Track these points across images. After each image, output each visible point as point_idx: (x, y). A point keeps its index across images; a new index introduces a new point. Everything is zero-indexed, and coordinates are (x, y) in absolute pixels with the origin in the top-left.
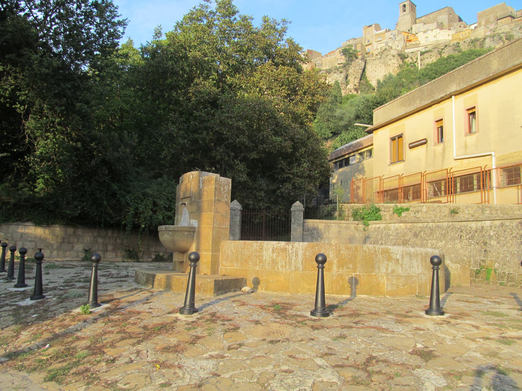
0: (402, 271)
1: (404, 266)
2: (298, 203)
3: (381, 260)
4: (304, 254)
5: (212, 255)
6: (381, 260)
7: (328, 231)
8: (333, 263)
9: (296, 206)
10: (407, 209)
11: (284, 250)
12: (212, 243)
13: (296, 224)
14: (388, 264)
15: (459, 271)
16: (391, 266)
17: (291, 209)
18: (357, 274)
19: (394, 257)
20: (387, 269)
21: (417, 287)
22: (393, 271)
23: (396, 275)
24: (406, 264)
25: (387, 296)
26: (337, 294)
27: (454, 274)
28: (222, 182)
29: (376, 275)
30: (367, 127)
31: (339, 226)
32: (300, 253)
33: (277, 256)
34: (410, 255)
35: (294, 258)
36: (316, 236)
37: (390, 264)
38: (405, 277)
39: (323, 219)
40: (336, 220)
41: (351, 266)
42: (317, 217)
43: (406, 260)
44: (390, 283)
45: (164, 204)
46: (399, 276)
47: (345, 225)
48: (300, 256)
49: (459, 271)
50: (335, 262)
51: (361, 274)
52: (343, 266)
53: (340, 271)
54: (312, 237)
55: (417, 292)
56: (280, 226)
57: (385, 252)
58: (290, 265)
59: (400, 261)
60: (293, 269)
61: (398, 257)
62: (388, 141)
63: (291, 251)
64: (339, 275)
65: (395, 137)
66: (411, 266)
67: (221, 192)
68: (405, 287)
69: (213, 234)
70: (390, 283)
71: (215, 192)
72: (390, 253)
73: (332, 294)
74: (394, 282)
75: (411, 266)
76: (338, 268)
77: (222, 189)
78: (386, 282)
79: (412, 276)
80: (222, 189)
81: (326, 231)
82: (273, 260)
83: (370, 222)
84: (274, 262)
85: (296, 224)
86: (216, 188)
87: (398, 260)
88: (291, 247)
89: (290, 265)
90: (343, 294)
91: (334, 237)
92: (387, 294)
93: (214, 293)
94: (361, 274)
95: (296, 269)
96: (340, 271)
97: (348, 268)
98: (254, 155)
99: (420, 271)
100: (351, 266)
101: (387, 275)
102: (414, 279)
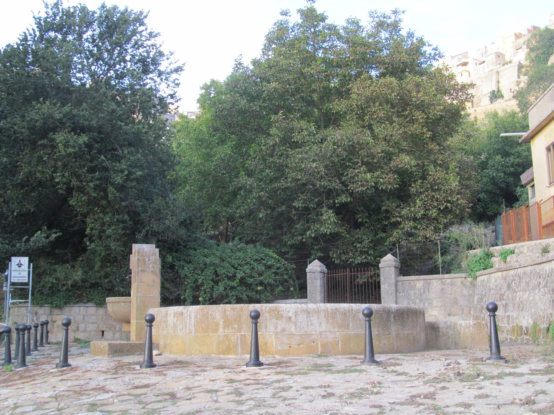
0: (296, 329)
1: (298, 325)
2: (389, 257)
3: (269, 318)
4: (196, 317)
5: (136, 323)
6: (269, 318)
7: (428, 290)
8: (219, 324)
9: (385, 261)
10: (513, 252)
11: (181, 314)
12: (137, 311)
13: (387, 284)
14: (277, 323)
15: (471, 329)
16: (281, 324)
17: (380, 265)
18: (243, 333)
19: (284, 315)
20: (276, 328)
21: (319, 345)
22: (284, 330)
23: (288, 333)
24: (302, 322)
25: (276, 356)
26: (223, 354)
27: (464, 334)
28: (146, 253)
29: (263, 334)
30: (522, 136)
31: (442, 282)
32: (193, 316)
33: (177, 320)
34: (308, 312)
35: (188, 321)
36: (412, 297)
37: (280, 322)
38: (301, 335)
39: (411, 275)
40: (439, 274)
41: (236, 326)
42: (167, 280)
43: (302, 318)
44: (280, 342)
45: (226, 273)
46: (291, 335)
47: (449, 281)
48: (192, 319)
49: (471, 329)
50: (221, 323)
51: (246, 334)
52: (228, 327)
53: (226, 331)
54: (408, 299)
55: (320, 351)
56: (372, 289)
57: (273, 311)
58: (185, 329)
59: (293, 319)
60: (188, 332)
61: (290, 314)
62: (544, 152)
63: (186, 315)
64: (225, 335)
65: (549, 146)
66: (310, 324)
67: (145, 263)
68: (301, 346)
69: (137, 303)
70: (280, 342)
71: (138, 263)
72: (279, 311)
73: (219, 354)
74: (286, 340)
75: (310, 324)
76: (224, 328)
77: (147, 260)
78: (274, 341)
79: (311, 334)
80: (147, 260)
81: (426, 290)
82: (174, 324)
83: (478, 273)
84: (175, 326)
85: (387, 284)
86: (139, 259)
87: (290, 318)
88: (186, 310)
89: (185, 329)
90: (229, 354)
91: (436, 298)
92: (276, 353)
93: (109, 355)
94: (246, 334)
95: (190, 332)
96: (226, 331)
97: (233, 328)
98: (344, 199)
99: (324, 328)
100: (236, 326)
101: (276, 334)
102: (314, 337)
